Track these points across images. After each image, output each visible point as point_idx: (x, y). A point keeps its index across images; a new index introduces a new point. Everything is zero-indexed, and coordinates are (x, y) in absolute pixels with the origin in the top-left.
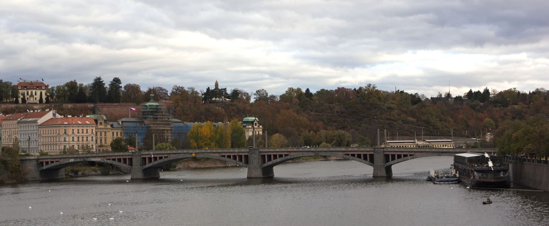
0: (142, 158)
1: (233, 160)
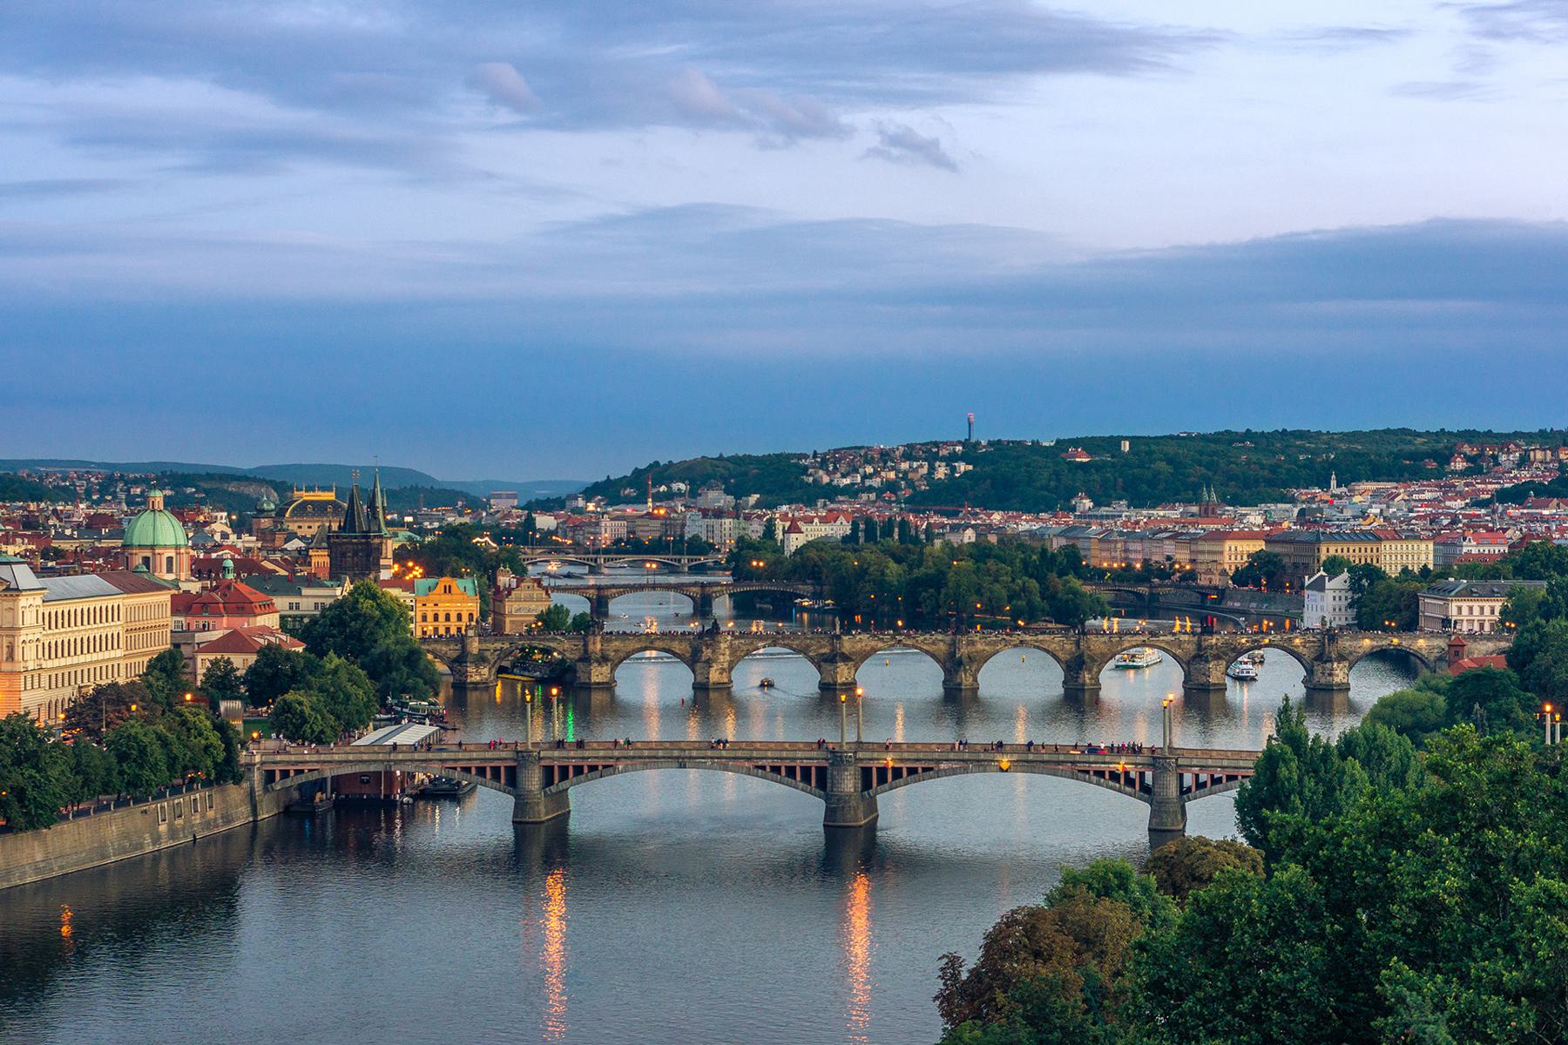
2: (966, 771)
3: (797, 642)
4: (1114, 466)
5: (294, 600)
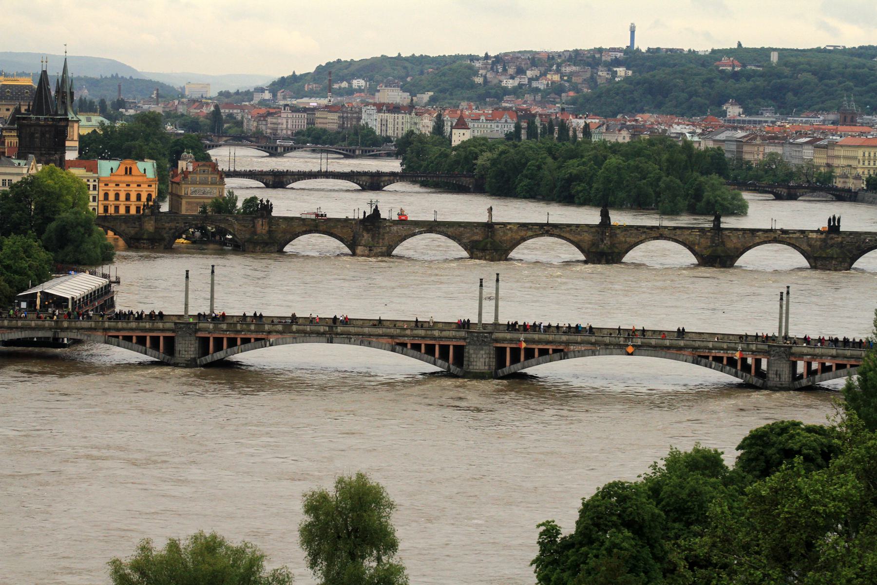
0: (200, 337)
1: (426, 356)
2: (594, 353)
3: (451, 230)
4: (762, 75)
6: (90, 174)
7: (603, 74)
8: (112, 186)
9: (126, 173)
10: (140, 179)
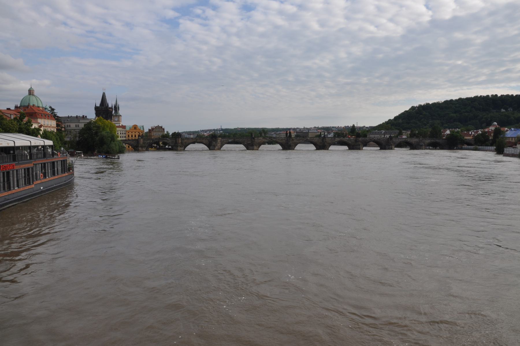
5: (77, 124)
6: (124, 129)
7: (218, 132)
8: (130, 133)
9: (135, 129)
10: (139, 131)
